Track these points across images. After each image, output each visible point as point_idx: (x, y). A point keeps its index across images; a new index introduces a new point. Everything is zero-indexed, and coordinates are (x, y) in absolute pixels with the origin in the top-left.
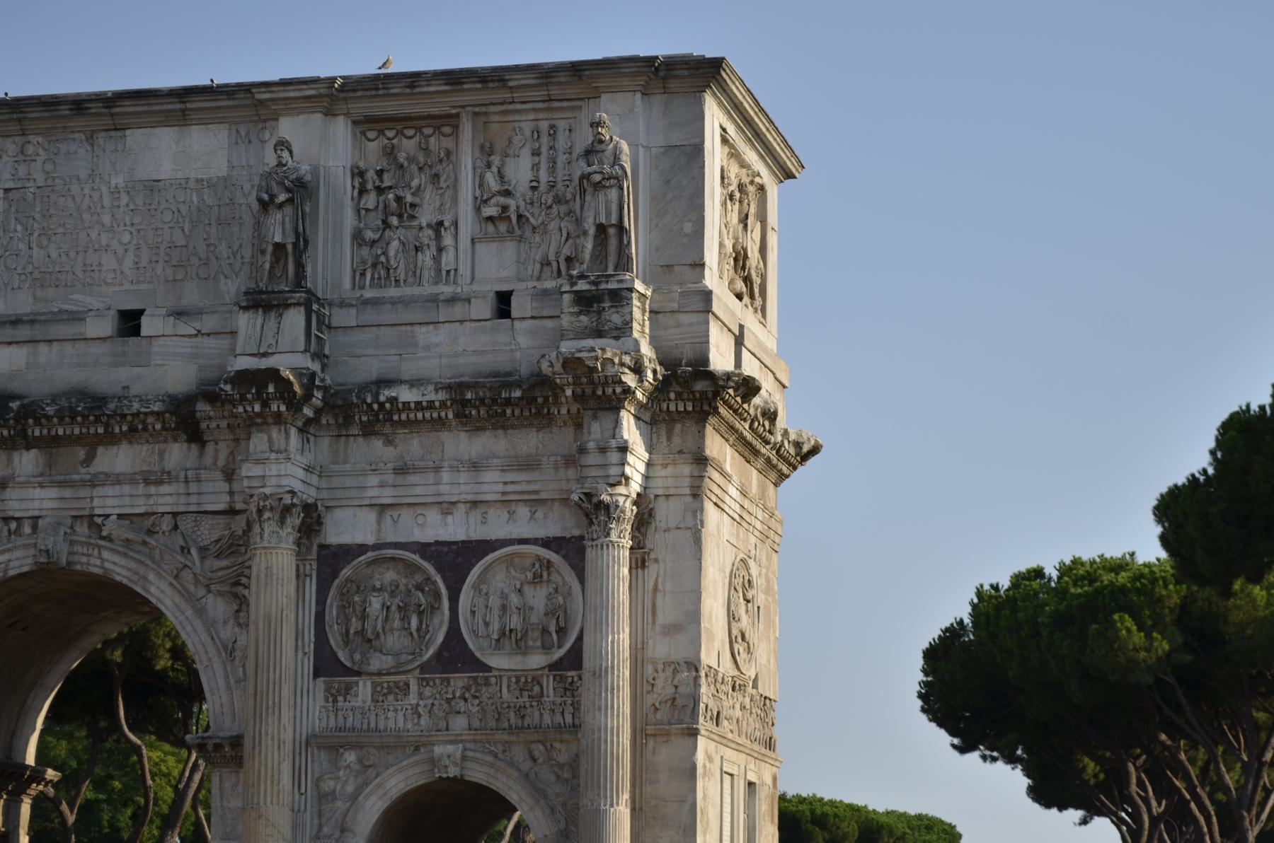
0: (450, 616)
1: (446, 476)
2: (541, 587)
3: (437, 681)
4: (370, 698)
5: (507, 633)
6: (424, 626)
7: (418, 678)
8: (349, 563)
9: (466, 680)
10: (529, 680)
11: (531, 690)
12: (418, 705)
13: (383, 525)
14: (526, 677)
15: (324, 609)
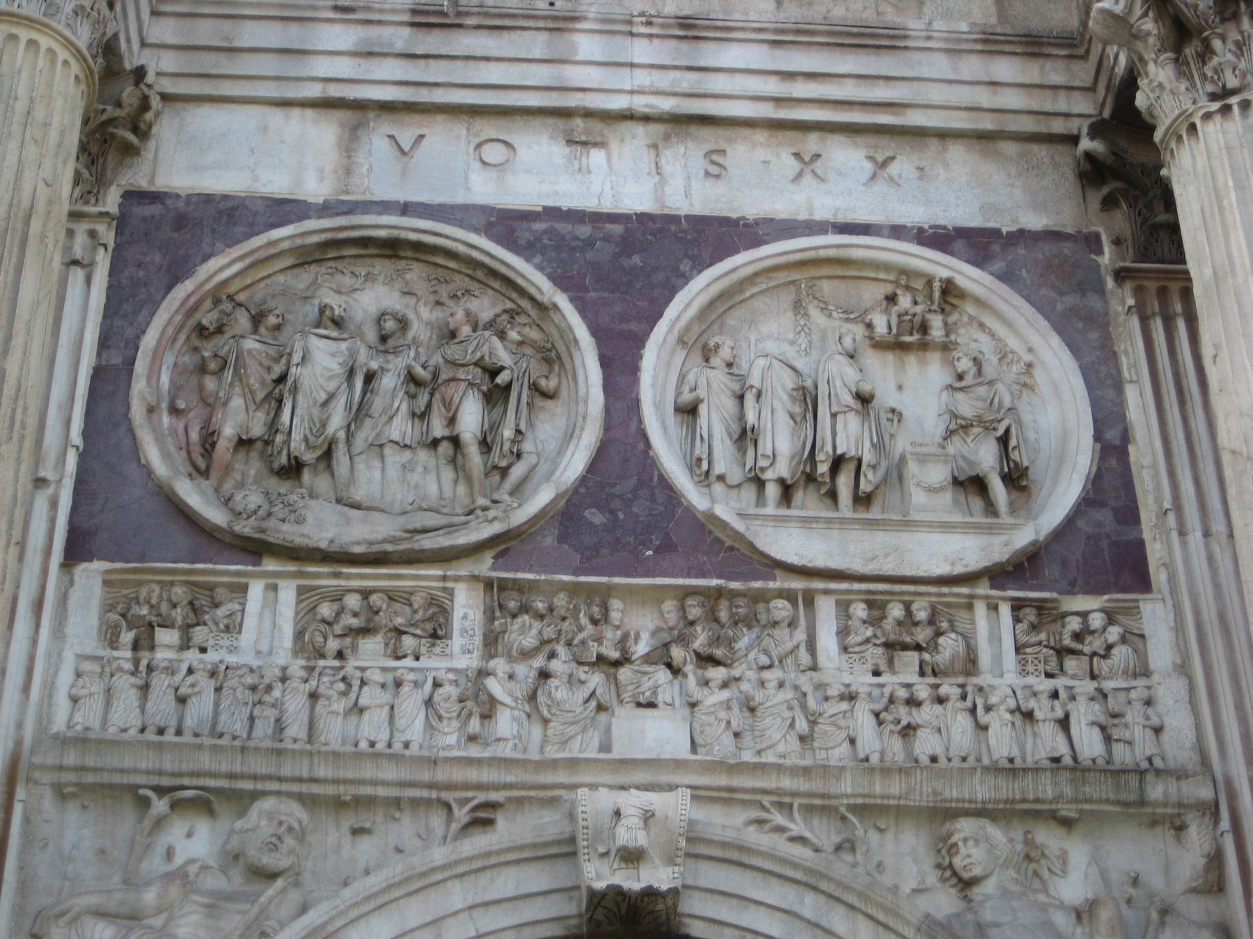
0: (608, 410)
1: (587, 45)
2: (923, 363)
3: (561, 601)
4: (287, 640)
5: (823, 468)
6: (508, 433)
7: (489, 584)
8: (232, 242)
9: (669, 606)
10: (922, 615)
11: (933, 646)
12: (483, 673)
13: (361, 157)
14: (907, 607)
15: (130, 362)
